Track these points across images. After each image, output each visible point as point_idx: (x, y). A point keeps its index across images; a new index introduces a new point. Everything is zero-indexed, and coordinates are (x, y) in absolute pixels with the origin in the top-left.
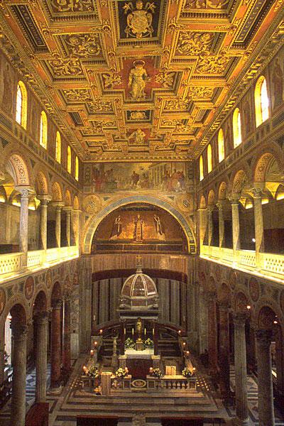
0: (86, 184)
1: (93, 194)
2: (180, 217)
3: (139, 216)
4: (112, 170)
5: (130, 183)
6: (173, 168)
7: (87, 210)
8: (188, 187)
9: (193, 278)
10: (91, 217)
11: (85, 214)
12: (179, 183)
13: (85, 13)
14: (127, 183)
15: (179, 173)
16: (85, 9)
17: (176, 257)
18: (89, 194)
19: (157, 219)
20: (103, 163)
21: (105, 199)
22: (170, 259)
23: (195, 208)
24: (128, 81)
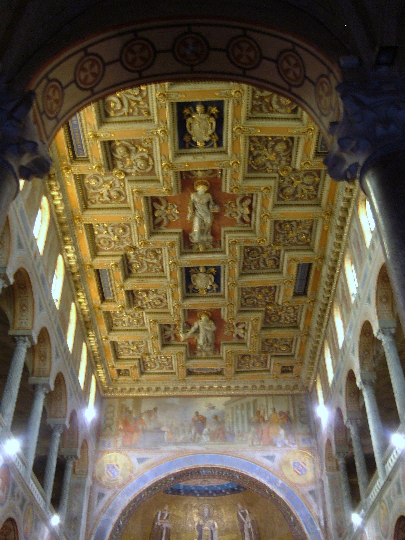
3: (206, 511)
4: (155, 409)
5: (190, 431)
6: (270, 406)
13: (140, 118)
14: (184, 431)
15: (281, 413)
16: (140, 113)
19: (244, 514)
20: (140, 398)
24: (186, 213)
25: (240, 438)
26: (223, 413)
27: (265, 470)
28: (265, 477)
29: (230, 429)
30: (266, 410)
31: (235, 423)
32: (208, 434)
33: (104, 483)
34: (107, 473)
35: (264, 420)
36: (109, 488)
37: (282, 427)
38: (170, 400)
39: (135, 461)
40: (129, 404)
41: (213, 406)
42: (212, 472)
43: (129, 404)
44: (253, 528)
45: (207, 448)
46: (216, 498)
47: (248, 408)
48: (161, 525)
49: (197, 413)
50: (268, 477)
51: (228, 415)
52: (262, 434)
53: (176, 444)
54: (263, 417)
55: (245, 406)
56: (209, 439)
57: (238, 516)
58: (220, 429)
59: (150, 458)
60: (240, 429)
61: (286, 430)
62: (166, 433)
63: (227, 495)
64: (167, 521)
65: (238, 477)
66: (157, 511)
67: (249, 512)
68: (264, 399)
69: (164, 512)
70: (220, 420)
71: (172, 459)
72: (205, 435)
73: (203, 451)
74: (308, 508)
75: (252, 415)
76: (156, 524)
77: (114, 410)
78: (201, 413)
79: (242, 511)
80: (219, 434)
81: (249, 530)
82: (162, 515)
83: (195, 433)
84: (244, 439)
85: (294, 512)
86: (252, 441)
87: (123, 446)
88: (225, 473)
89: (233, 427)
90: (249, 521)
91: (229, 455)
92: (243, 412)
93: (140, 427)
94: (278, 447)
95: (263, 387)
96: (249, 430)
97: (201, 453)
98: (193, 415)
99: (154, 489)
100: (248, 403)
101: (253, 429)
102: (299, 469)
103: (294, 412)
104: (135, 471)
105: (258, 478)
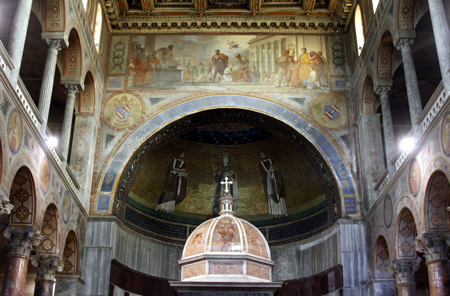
0: (114, 72)
1: (128, 92)
2: (321, 139)
3: (226, 160)
4: (171, 47)
5: (210, 70)
6: (301, 46)
7: (113, 122)
8: (333, 80)
9: (356, 273)
10: (118, 136)
11: (107, 131)
12: (313, 74)
15: (312, 54)
17: (312, 244)
18: (119, 92)
19: (267, 164)
21: (154, 101)
22: (299, 253)
23: (352, 121)
25: (266, 79)
26: (247, 52)
27: (294, 113)
28: (293, 120)
29: (254, 69)
31: (260, 63)
32: (229, 74)
33: (113, 124)
34: (116, 114)
35: (293, 61)
36: (118, 130)
37: (313, 69)
38: (187, 38)
39: (147, 102)
40: (141, 41)
41: (236, 44)
42: (233, 115)
43: (141, 41)
44: (276, 179)
45: (229, 89)
46: (236, 146)
47: (276, 48)
48: (177, 174)
49: (218, 51)
50: (296, 121)
51: (253, 54)
52: (291, 75)
53: (193, 84)
54: (292, 58)
55: (272, 46)
56: (231, 79)
57: (261, 166)
58: (244, 69)
59: (164, 99)
60: (266, 69)
61: (317, 71)
62: (182, 72)
63: (250, 142)
64: (182, 170)
65: (262, 120)
66: (173, 159)
67: (273, 162)
68: (294, 37)
69: (180, 160)
70: (243, 59)
71: (189, 100)
72: (227, 75)
73: (224, 91)
74: (340, 155)
75: (280, 55)
76: (171, 172)
77: (124, 48)
79: (265, 161)
80: (242, 74)
81: (272, 180)
82: (178, 163)
83: (216, 73)
84: (269, 80)
85: (324, 158)
86: (280, 83)
87: (134, 86)
88: (248, 116)
89: (258, 67)
90: (273, 171)
91: (254, 97)
92: (270, 51)
93: (153, 66)
94: (308, 89)
95: (293, 25)
96: (276, 72)
97: (222, 94)
98: (214, 53)
99: (169, 132)
100: (276, 42)
101: (280, 70)
102: (331, 113)
104: (148, 113)
105: (285, 121)
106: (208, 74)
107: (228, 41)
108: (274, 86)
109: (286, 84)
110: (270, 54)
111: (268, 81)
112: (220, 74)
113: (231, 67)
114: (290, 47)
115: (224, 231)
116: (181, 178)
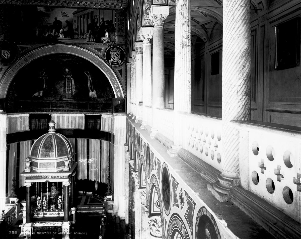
5: (52, 32)
30: (98, 19)
41: (66, 14)
47: (88, 18)
49: (56, 18)
56: (63, 36)
72: (61, 34)
78: (58, 19)
86: (89, 39)
96: (88, 32)
98: (54, 20)
103: (115, 21)
106: (51, 33)
107: (62, 12)
108: (86, 41)
109: (93, 40)
110: (84, 21)
111: (83, 38)
112: (57, 33)
113: (63, 29)
114: (96, 17)
115: (47, 146)
116: (44, 80)
